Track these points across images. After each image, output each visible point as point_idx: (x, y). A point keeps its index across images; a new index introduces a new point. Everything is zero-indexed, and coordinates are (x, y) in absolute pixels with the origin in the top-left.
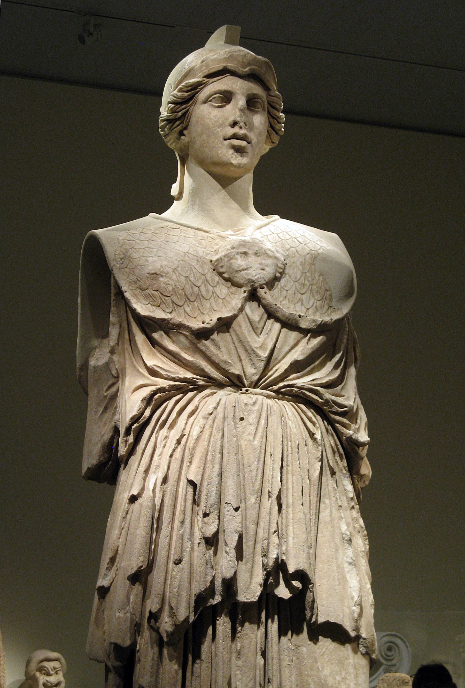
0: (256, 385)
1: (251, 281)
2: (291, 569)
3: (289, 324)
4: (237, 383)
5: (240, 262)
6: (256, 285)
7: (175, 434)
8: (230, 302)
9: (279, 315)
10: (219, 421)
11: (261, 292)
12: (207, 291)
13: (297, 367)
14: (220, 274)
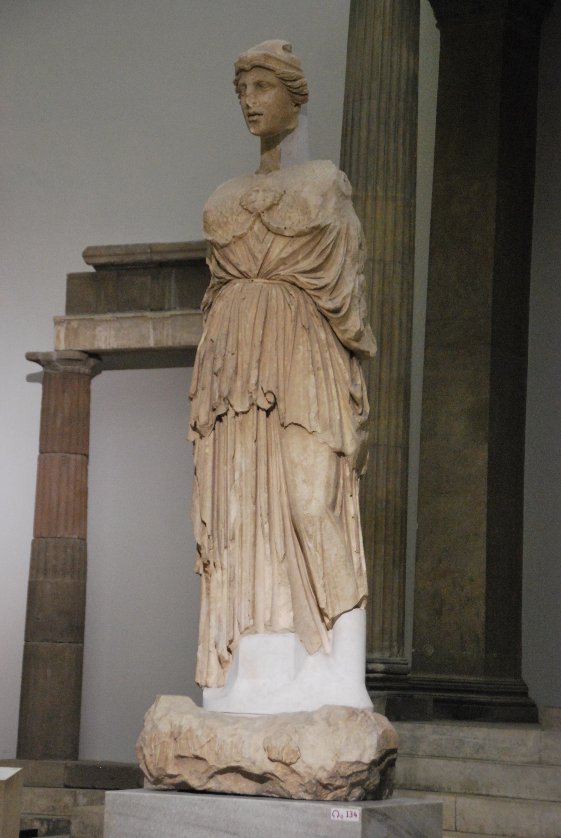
4: (245, 275)
6: (259, 211)
12: (232, 219)
13: (283, 262)
14: (243, 206)
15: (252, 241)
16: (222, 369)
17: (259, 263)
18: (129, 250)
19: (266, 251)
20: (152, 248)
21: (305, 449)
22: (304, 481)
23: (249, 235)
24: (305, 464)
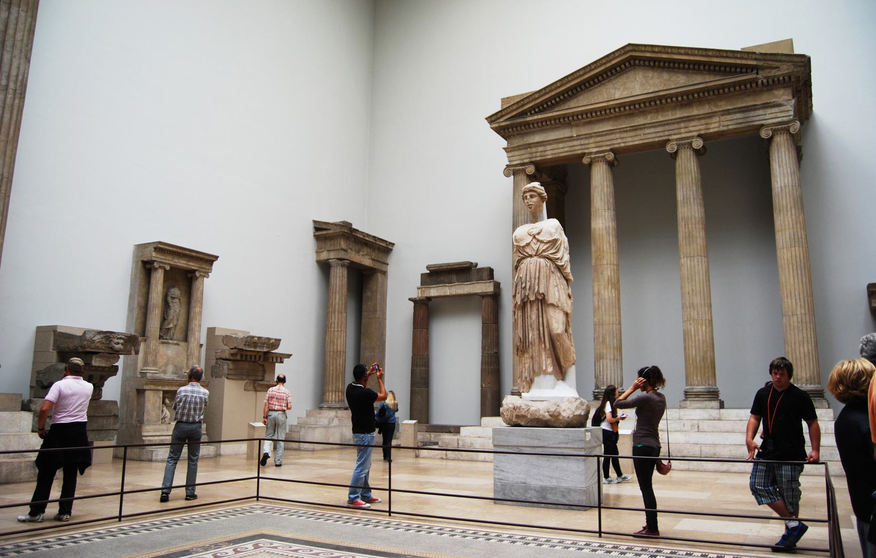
3: (542, 242)
4: (531, 256)
13: (544, 251)
15: (532, 244)
16: (525, 287)
18: (441, 266)
20: (448, 265)
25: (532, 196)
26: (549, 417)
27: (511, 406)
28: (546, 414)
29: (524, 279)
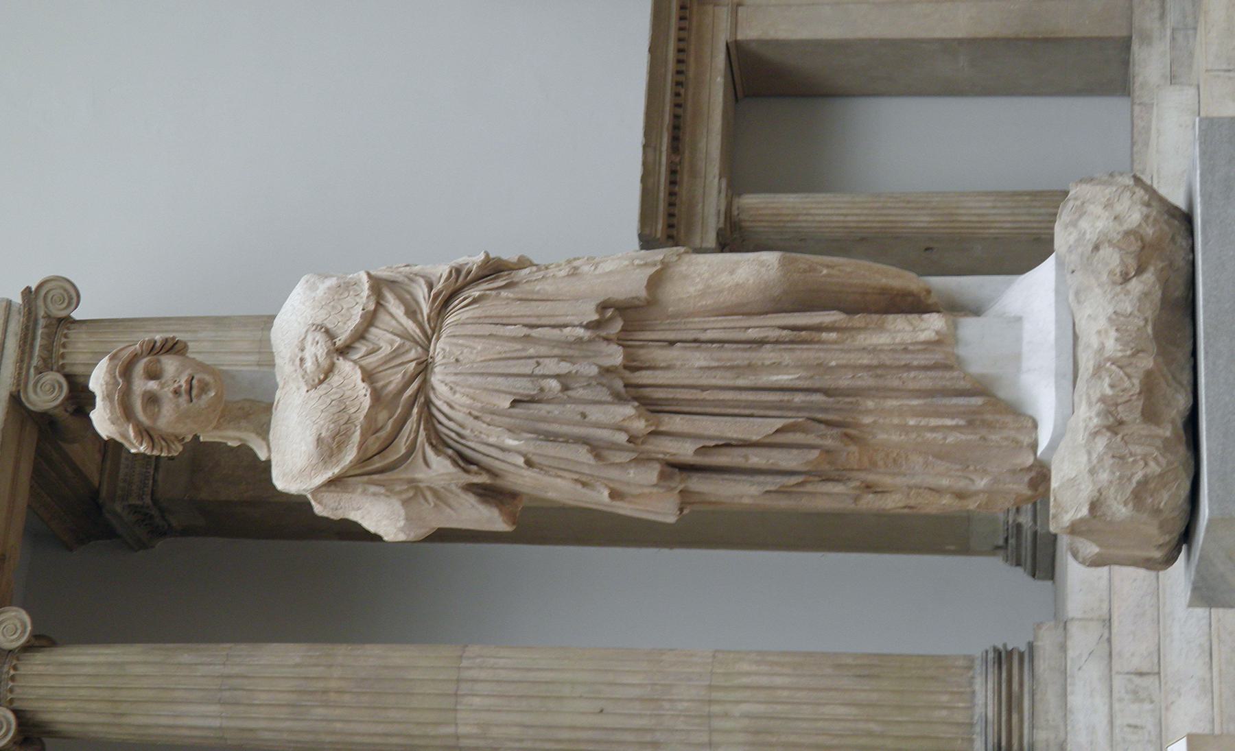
0: (427, 350)
1: (328, 354)
2: (596, 317)
3: (370, 320)
4: (424, 367)
5: (309, 364)
7: (470, 422)
8: (349, 372)
9: (361, 328)
10: (459, 379)
11: (339, 342)
13: (412, 313)
14: (321, 382)
15: (372, 360)
17: (408, 344)
19: (390, 336)
21: (685, 277)
22: (732, 272)
23: (363, 363)
24: (707, 275)
25: (154, 374)
26: (1149, 276)
27: (1101, 443)
28: (1136, 286)
29: (525, 387)
